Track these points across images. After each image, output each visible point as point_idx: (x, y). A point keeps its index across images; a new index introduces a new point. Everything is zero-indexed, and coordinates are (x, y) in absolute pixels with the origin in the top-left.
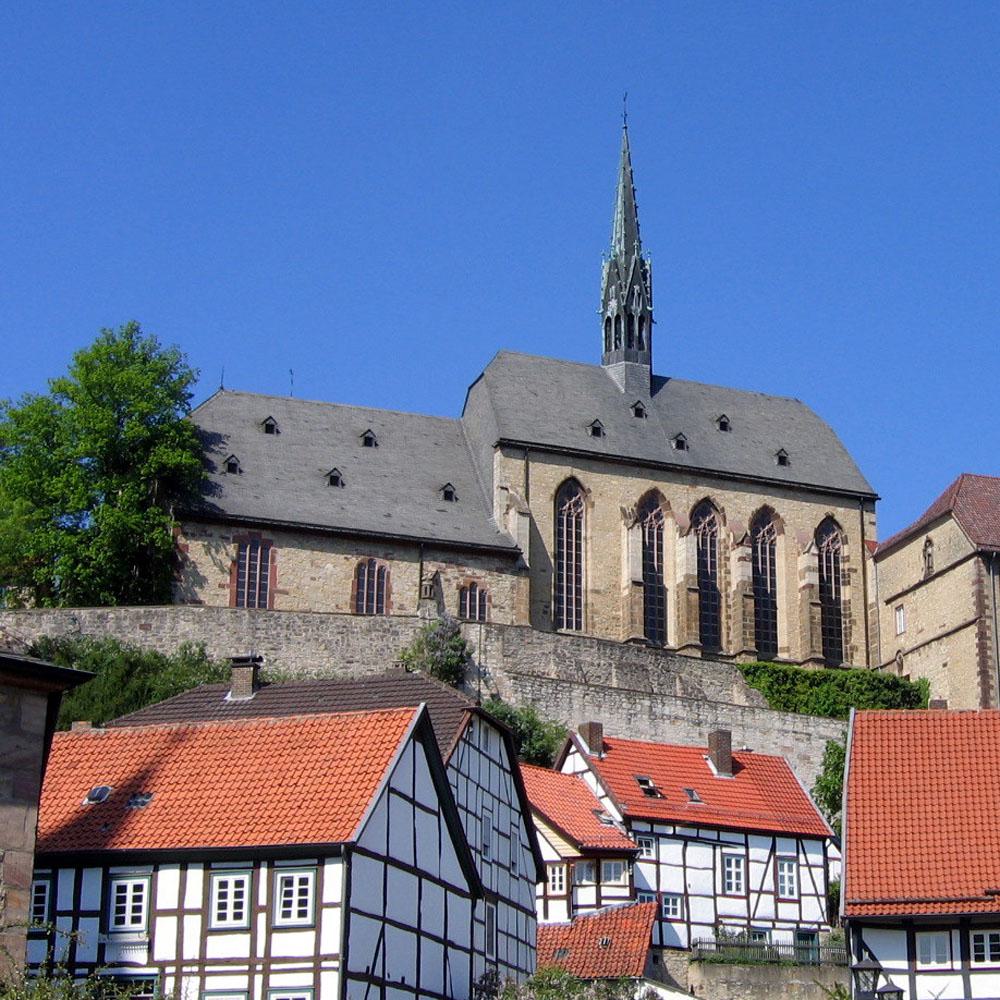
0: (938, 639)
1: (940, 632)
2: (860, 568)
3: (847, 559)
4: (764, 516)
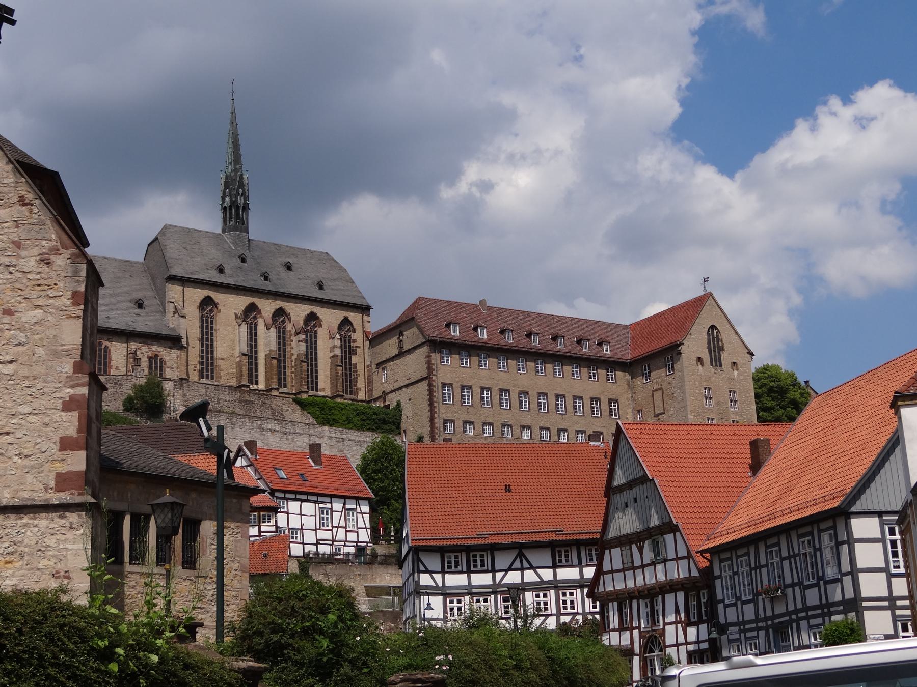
0: (407, 386)
1: (407, 382)
2: (362, 346)
3: (355, 341)
4: (312, 317)
